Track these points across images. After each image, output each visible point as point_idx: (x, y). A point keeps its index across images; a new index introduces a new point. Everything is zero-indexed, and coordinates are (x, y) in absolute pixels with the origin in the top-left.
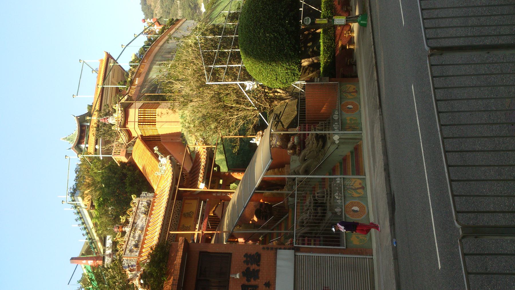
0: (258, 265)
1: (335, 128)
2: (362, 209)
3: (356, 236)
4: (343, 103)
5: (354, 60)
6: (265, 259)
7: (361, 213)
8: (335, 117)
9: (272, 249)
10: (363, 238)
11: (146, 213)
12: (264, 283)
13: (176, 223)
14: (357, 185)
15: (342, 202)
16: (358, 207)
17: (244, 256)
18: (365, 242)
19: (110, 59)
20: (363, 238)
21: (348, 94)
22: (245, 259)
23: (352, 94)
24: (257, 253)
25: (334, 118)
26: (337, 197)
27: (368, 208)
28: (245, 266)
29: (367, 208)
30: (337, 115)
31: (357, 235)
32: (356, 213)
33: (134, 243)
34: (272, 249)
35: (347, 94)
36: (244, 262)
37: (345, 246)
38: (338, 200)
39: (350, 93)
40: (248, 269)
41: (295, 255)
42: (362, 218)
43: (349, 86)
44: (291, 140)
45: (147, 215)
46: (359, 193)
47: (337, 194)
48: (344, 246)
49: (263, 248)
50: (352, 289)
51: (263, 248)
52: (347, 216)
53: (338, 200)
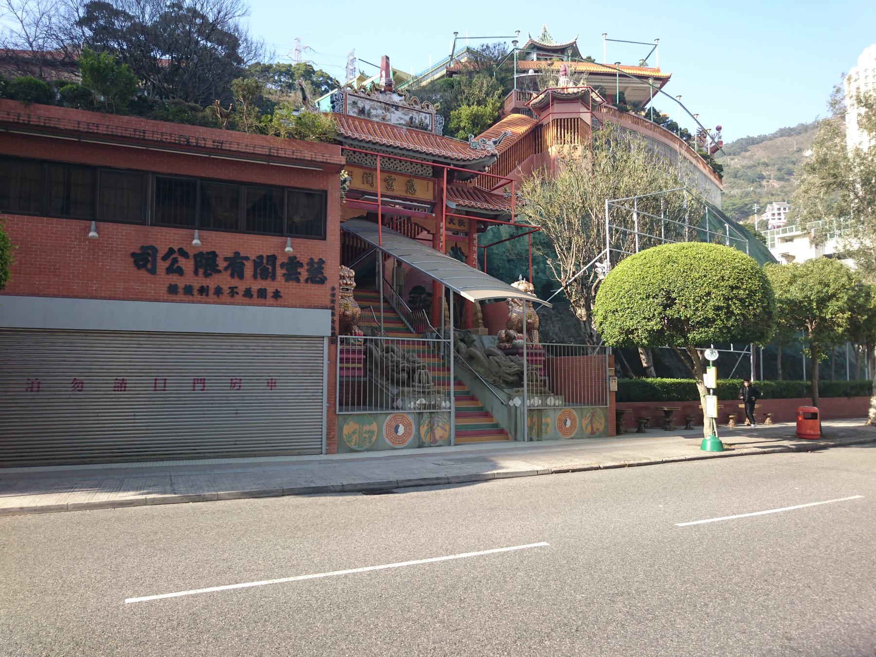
0: (307, 281)
1: (532, 400)
5: (647, 430)
6: (315, 290)
9: (333, 301)
10: (354, 441)
11: (411, 123)
12: (279, 290)
13: (398, 169)
14: (439, 432)
17: (321, 260)
19: (661, 82)
20: (354, 441)
22: (316, 260)
23: (589, 427)
24: (326, 279)
26: (418, 402)
27: (402, 449)
28: (304, 260)
31: (358, 431)
33: (367, 108)
34: (333, 301)
36: (312, 259)
37: (340, 413)
38: (415, 403)
40: (301, 265)
45: (410, 126)
49: (333, 289)
50: (1, 430)
51: (333, 289)
52: (389, 417)
53: (415, 403)
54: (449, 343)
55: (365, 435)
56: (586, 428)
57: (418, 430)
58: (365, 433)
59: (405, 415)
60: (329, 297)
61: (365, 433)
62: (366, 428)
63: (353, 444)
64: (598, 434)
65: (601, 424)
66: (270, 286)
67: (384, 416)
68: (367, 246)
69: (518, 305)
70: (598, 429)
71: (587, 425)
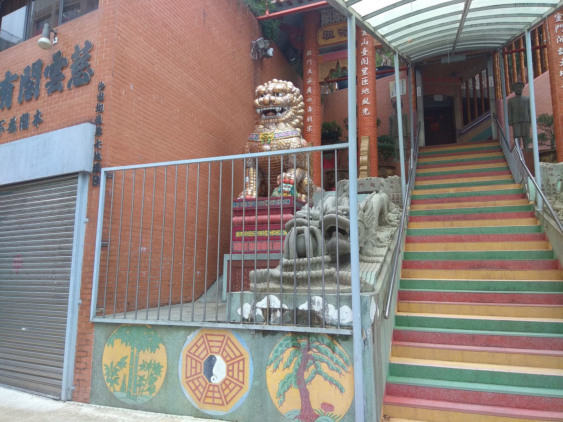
2: (217, 395)
3: (126, 357)
7: (201, 389)
10: (120, 381)
12: (40, 110)
15: (244, 321)
16: (224, 382)
17: (87, 43)
18: (108, 384)
20: (120, 381)
26: (263, 304)
28: (68, 53)
29: (221, 413)
31: (128, 360)
32: (200, 368)
34: (99, 109)
37: (97, 320)
38: (254, 308)
41: (72, 176)
42: (184, 389)
46: (282, 395)
47: (276, 302)
48: (98, 314)
49: (102, 87)
52: (192, 337)
54: (344, 152)
55: (141, 373)
57: (260, 375)
58: (143, 366)
59: (234, 337)
60: (95, 102)
61: (143, 366)
62: (145, 356)
63: (117, 388)
66: (31, 109)
67: (182, 333)
68: (411, 73)
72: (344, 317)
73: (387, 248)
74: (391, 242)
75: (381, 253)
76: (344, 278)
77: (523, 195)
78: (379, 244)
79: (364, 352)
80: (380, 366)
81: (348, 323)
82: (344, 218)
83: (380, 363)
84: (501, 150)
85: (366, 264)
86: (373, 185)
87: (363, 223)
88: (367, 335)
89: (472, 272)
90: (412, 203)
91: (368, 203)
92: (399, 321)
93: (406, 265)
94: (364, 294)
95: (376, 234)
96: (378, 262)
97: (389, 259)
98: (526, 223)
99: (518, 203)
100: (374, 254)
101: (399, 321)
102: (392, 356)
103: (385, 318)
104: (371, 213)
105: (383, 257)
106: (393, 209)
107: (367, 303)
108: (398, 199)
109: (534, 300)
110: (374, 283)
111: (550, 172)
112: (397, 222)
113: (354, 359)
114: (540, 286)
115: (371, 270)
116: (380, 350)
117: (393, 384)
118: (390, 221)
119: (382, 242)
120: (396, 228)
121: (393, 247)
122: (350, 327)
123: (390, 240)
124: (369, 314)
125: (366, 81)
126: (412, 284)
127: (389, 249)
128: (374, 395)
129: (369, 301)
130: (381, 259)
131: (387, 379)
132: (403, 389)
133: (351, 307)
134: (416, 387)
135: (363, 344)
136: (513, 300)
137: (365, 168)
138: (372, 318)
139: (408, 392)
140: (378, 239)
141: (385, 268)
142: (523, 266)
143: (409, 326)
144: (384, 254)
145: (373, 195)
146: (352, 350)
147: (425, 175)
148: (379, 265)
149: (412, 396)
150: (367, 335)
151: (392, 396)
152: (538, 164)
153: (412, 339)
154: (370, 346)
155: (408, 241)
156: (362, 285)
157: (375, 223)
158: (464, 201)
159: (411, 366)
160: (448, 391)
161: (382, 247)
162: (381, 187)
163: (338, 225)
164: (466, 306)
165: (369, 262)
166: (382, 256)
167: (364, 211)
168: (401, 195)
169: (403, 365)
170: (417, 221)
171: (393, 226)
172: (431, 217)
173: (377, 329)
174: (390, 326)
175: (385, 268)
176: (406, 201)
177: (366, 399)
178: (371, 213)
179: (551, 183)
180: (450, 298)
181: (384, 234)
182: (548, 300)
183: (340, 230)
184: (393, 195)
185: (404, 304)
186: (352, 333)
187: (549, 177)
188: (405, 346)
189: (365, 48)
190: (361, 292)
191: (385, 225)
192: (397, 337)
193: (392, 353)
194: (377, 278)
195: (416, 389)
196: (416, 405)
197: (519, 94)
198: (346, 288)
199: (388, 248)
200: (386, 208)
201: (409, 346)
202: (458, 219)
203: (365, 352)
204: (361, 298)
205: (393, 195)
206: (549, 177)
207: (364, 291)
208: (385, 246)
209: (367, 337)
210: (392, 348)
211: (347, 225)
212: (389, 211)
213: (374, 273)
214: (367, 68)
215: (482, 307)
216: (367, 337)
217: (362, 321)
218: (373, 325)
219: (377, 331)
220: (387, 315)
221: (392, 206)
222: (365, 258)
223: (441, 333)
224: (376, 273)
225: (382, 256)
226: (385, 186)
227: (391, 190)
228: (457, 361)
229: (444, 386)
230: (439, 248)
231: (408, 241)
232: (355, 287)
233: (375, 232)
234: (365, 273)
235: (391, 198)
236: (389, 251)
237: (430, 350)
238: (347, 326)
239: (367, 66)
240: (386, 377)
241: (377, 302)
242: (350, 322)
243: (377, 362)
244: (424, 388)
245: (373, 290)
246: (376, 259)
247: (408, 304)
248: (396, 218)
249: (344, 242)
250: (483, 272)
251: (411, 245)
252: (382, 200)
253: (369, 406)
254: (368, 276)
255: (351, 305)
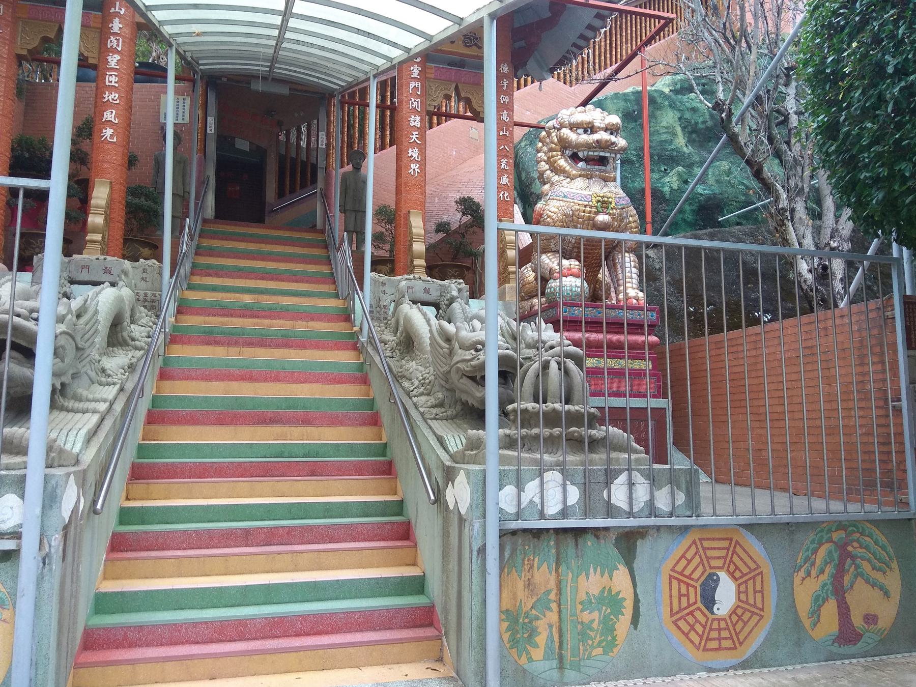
1: (531, 489)
4: (754, 545)
8: (631, 484)
21: (824, 578)
23: (830, 609)
25: (623, 478)
30: (651, 503)
35: (830, 570)
39: (839, 591)
43: (893, 581)
44: (565, 263)
56: (816, 613)
64: (869, 640)
65: (887, 594)
69: (568, 176)
70: (870, 619)
71: (818, 603)
72: (6, 517)
73: (118, 386)
74: (128, 377)
75: (105, 396)
76: (15, 441)
77: (346, 316)
78: (104, 380)
79: (40, 579)
80: (73, 601)
81: (14, 527)
82: (30, 325)
83: (75, 596)
84: (326, 247)
85: (71, 415)
86: (108, 271)
87: (73, 338)
88: (50, 546)
89: (261, 430)
90: (180, 311)
91: (88, 302)
92: (125, 516)
93: (153, 418)
94: (50, 471)
95: (99, 361)
96: (94, 412)
97: (118, 407)
98: (344, 358)
99: (338, 327)
100: (91, 397)
101: (125, 516)
102: (105, 578)
103: (96, 512)
104: (93, 321)
105: (108, 404)
106: (142, 318)
107: (57, 485)
108: (153, 301)
109: (341, 470)
110: (81, 451)
111: (382, 288)
112: (145, 342)
113: (18, 594)
114: (352, 449)
115: (78, 426)
116: (78, 571)
117: (97, 629)
118: (133, 340)
119: (109, 376)
120: (142, 352)
121: (129, 386)
122: (16, 535)
123: (127, 374)
124: (60, 507)
125: (113, 79)
126: (159, 450)
127: (122, 389)
128: (52, 654)
129: (60, 483)
130: (103, 407)
131: (87, 620)
132: (115, 635)
133: (22, 497)
134: (140, 628)
135: (41, 564)
136: (314, 471)
137: (98, 237)
138: (66, 515)
139: (125, 638)
140: (104, 370)
141: (108, 424)
142: (333, 420)
143: (143, 523)
144: (111, 397)
145: (103, 289)
146: (15, 578)
147: (209, 266)
148: (95, 418)
149: (132, 645)
150: (50, 546)
151: (93, 650)
152: (369, 275)
153: (145, 546)
154: (54, 567)
155: (164, 375)
156: (53, 455)
157: (100, 340)
158: (265, 317)
159: (136, 593)
160: (194, 627)
161: (108, 384)
162: (123, 277)
163: (12, 335)
164: (243, 483)
165: (77, 411)
166: (105, 401)
167: (79, 316)
168: (160, 295)
169: (122, 594)
170: (185, 343)
171: (137, 348)
172: (209, 338)
173: (75, 534)
174: (108, 524)
175: (108, 424)
176: (169, 309)
177: (35, 665)
178: (93, 321)
179: (382, 303)
180: (221, 471)
181: (117, 361)
182: (359, 469)
183: (15, 347)
184: (146, 295)
185: (140, 487)
186: (19, 545)
187: (381, 295)
188: (129, 559)
189: (117, 20)
190: (47, 467)
191: (121, 346)
192: (118, 544)
193: (105, 573)
194: (89, 440)
195: (139, 632)
196: (134, 660)
197: (357, 168)
198: (18, 459)
199: (120, 387)
200: (127, 315)
201: (136, 559)
202: (251, 344)
203: (43, 578)
204: (47, 479)
205: (146, 295)
206: (381, 295)
207: (56, 464)
208: (114, 384)
209: (50, 550)
210: (105, 566)
211: (32, 338)
212: (133, 322)
213: (83, 432)
214: (118, 57)
215: (268, 483)
216: (50, 550)
217: (42, 521)
218: (66, 528)
219: (75, 538)
220: (99, 507)
221: (140, 313)
222: (70, 404)
223: (196, 531)
224: (89, 432)
225: (105, 401)
226: (131, 275)
227: (143, 285)
228: (217, 575)
229: (188, 619)
230: (215, 390)
231: (164, 375)
232: (36, 458)
233: (97, 357)
234: (65, 432)
235: (141, 298)
236: (121, 393)
237: (173, 560)
238: (10, 533)
239: (118, 52)
240: (84, 617)
241: (82, 482)
242: (18, 525)
243: (67, 594)
244: (155, 627)
245: (77, 462)
246: (92, 405)
247: (146, 485)
248: (144, 334)
249: (26, 371)
250: (277, 429)
251: (167, 384)
252: (120, 300)
253: (40, 677)
254: (71, 437)
255: (23, 493)
